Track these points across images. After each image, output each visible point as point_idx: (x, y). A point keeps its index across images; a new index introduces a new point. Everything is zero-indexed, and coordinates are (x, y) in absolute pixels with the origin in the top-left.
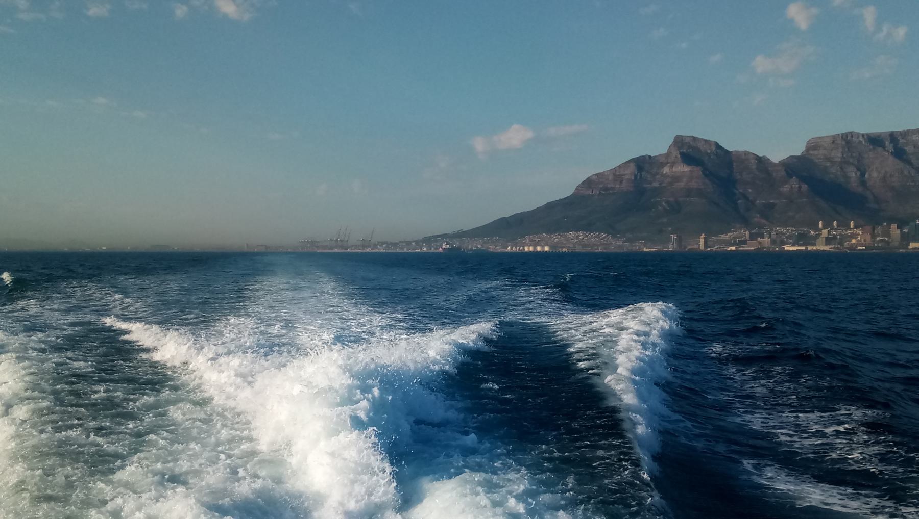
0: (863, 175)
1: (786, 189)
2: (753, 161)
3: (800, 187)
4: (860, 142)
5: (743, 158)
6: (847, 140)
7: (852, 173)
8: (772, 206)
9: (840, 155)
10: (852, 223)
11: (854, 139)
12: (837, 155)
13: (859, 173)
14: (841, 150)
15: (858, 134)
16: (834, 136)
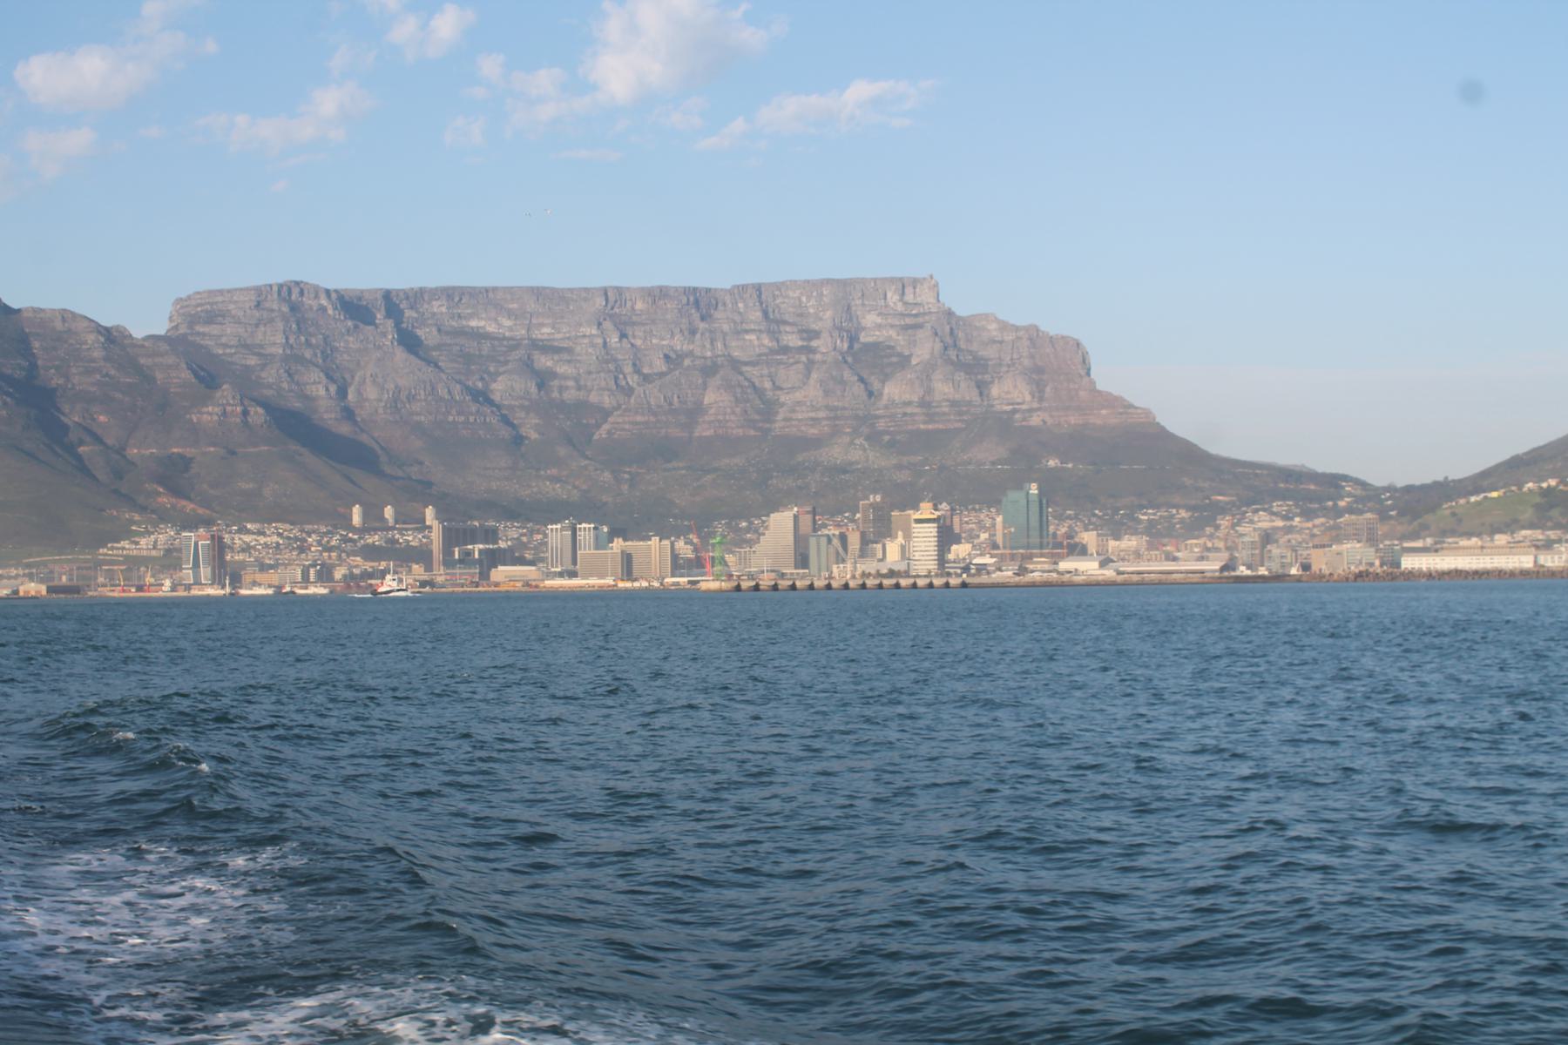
0: (342, 392)
1: (208, 415)
2: (91, 338)
3: (245, 413)
4: (323, 309)
5: (63, 330)
6: (292, 300)
7: (319, 389)
8: (186, 462)
9: (280, 339)
10: (389, 512)
11: (308, 301)
12: (274, 339)
13: (333, 389)
14: (280, 325)
15: (317, 290)
16: (258, 290)
